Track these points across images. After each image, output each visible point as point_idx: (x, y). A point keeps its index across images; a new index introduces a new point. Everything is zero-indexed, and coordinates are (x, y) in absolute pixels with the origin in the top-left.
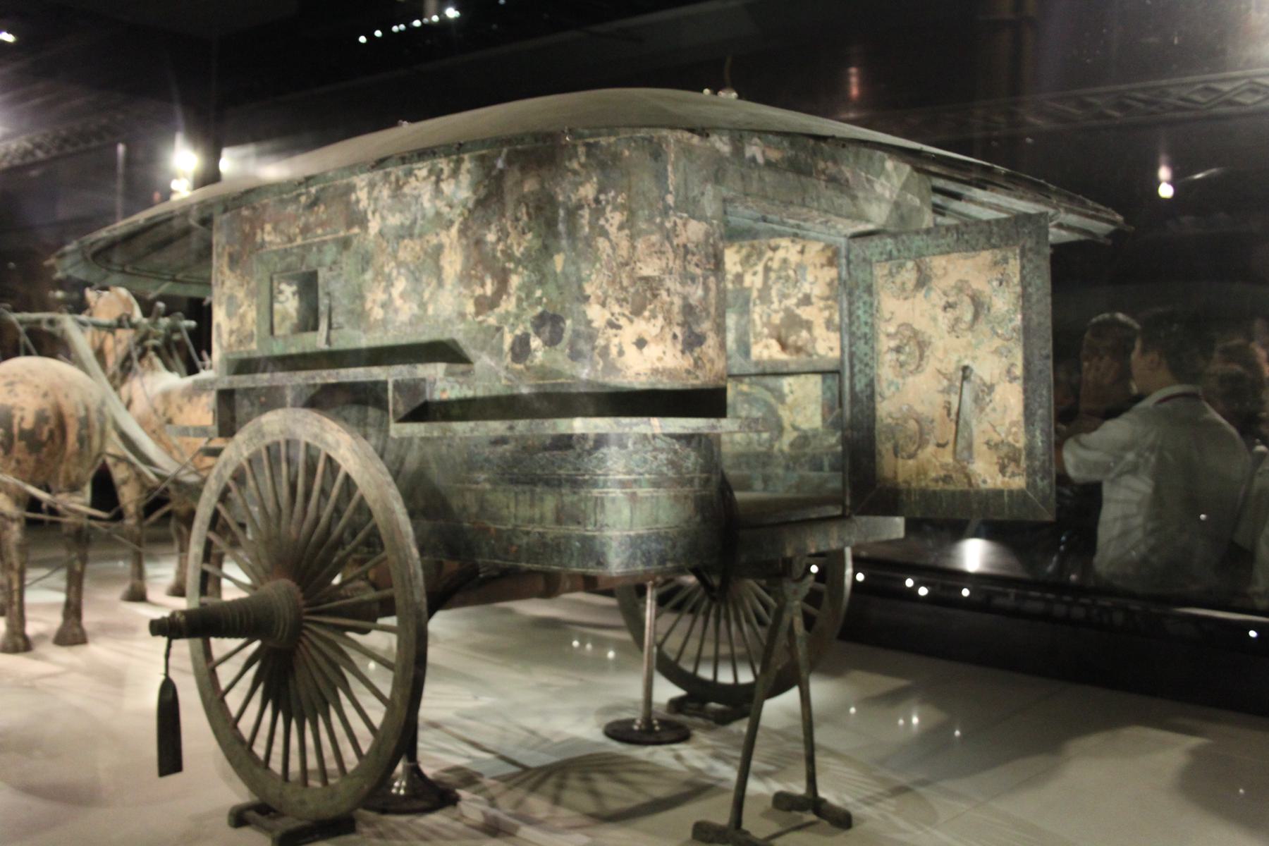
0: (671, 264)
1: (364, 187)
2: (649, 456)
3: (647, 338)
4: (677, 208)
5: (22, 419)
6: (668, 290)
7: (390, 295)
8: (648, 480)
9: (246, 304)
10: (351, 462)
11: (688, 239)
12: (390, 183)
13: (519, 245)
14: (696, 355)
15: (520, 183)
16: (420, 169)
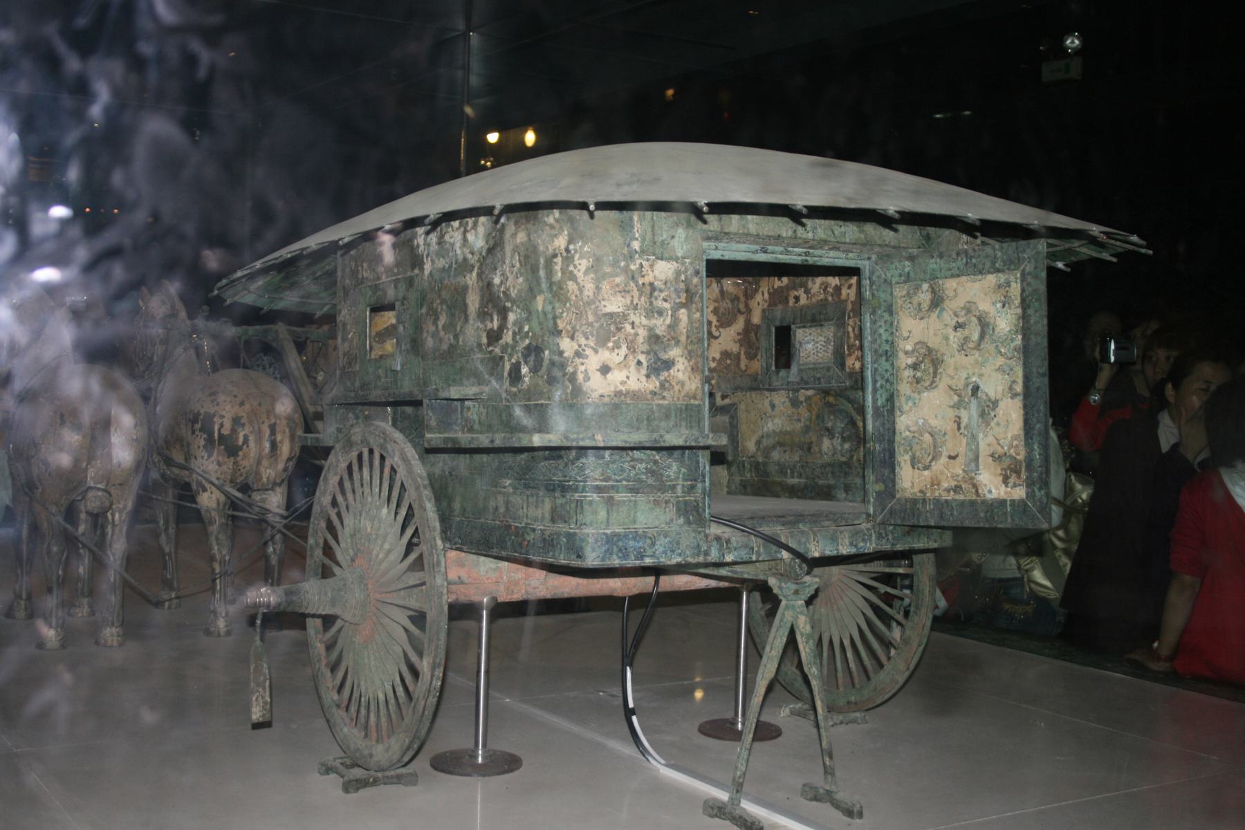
0: (635, 302)
2: (626, 466)
3: (611, 365)
4: (643, 252)
5: (222, 425)
6: (633, 323)
8: (627, 486)
11: (655, 277)
14: (662, 378)
15: (514, 235)
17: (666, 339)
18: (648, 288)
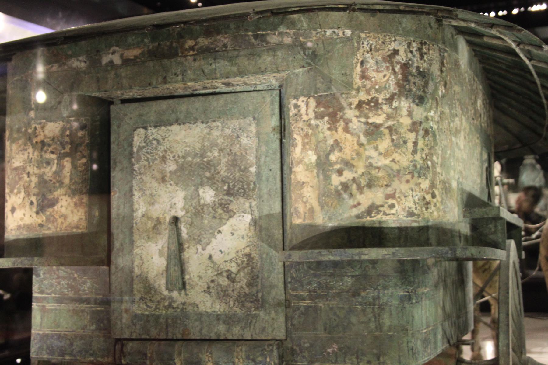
0: (31, 156)
6: (28, 174)
8: (54, 297)
11: (45, 136)
14: (48, 213)
17: (52, 182)
18: (40, 145)
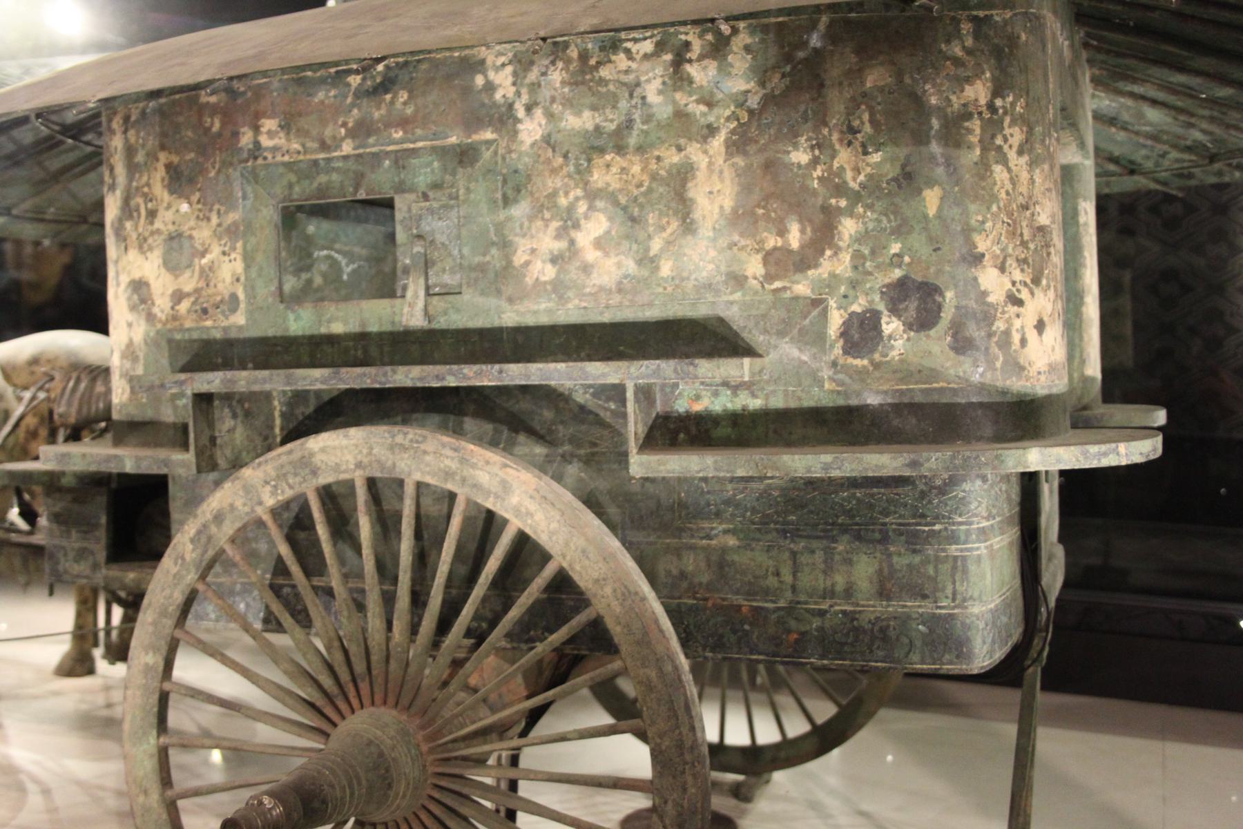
1: (503, 65)
7: (572, 242)
9: (216, 251)
10: (539, 516)
12: (568, 61)
13: (857, 171)
15: (856, 74)
16: (635, 40)
